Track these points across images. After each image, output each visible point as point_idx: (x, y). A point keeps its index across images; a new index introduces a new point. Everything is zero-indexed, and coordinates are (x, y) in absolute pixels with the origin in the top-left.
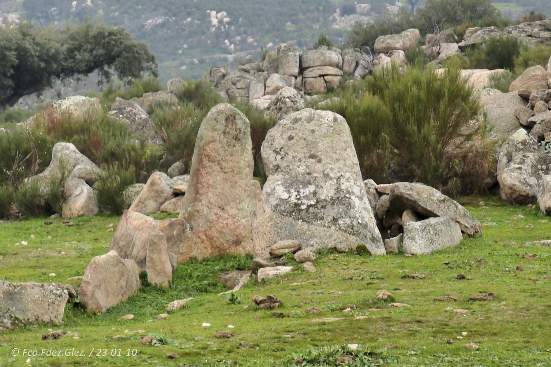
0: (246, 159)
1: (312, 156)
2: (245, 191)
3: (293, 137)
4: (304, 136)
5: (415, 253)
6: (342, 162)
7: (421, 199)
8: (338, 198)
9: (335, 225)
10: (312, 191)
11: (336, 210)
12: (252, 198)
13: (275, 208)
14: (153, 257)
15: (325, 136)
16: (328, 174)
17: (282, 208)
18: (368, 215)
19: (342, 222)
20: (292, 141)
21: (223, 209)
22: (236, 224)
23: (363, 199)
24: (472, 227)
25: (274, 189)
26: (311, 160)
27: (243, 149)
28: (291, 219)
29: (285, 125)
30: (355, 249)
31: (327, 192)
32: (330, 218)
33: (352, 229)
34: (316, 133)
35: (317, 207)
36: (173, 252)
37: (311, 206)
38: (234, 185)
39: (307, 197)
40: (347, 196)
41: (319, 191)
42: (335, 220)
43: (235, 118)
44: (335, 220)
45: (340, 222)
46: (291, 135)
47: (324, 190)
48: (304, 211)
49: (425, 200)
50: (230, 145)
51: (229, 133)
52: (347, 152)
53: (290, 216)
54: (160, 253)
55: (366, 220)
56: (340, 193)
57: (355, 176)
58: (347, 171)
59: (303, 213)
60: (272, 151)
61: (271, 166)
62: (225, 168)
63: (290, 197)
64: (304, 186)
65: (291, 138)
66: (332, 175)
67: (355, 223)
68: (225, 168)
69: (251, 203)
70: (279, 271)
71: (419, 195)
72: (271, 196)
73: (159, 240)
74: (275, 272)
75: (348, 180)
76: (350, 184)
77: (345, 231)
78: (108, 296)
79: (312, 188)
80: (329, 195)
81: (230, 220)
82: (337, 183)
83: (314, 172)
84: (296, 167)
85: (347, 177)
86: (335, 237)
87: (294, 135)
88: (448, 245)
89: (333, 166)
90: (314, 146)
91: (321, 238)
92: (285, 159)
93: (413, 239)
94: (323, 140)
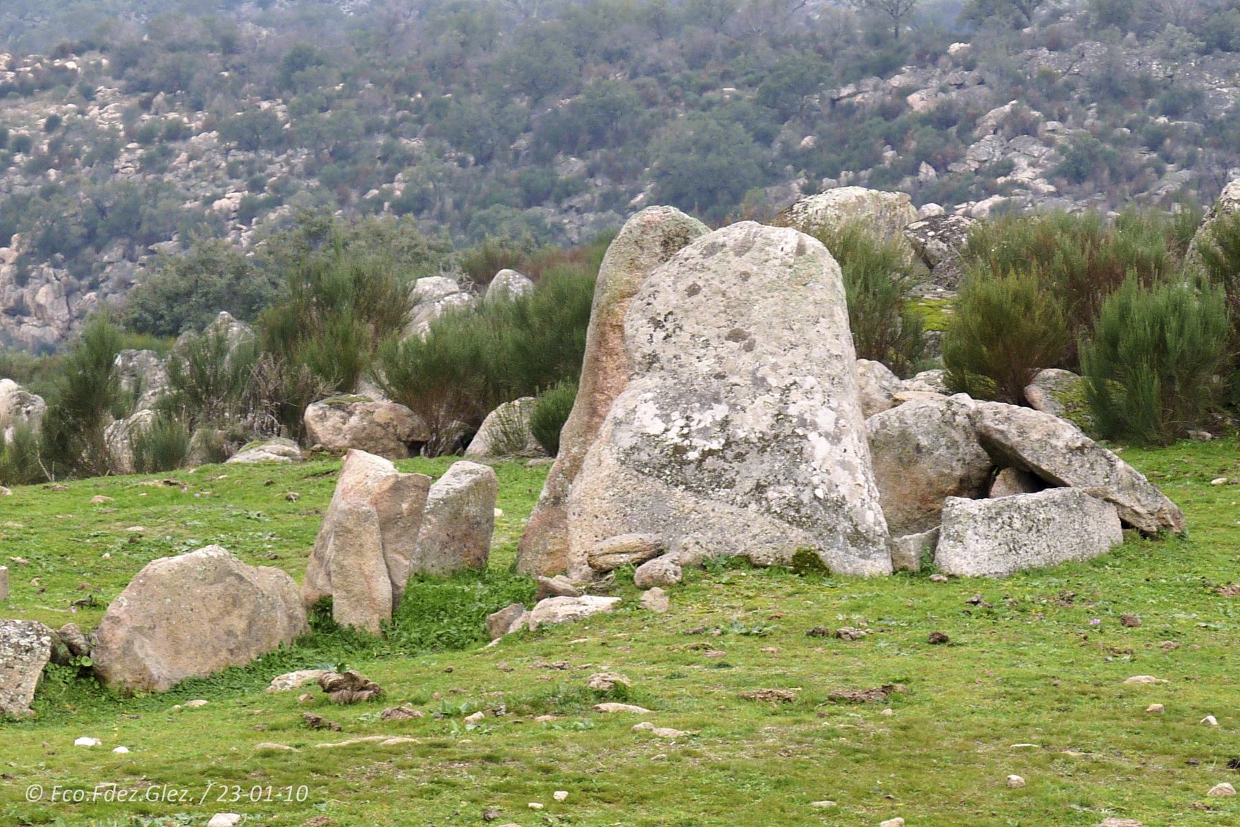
1: (736, 336)
3: (700, 288)
4: (723, 287)
5: (958, 573)
6: (802, 350)
7: (1027, 443)
8: (776, 436)
9: (758, 501)
10: (718, 418)
11: (766, 466)
13: (628, 455)
14: (345, 563)
15: (772, 287)
16: (763, 379)
17: (644, 457)
18: (849, 480)
19: (776, 495)
20: (695, 299)
23: (839, 440)
25: (634, 411)
26: (731, 344)
28: (659, 484)
29: (686, 259)
30: (790, 560)
31: (754, 420)
32: (749, 484)
33: (798, 511)
34: (753, 279)
35: (724, 458)
36: (400, 553)
37: (711, 452)
39: (705, 432)
40: (800, 431)
41: (736, 418)
42: (760, 488)
44: (760, 488)
45: (771, 494)
46: (695, 284)
47: (749, 416)
48: (693, 466)
49: (1036, 445)
53: (659, 477)
54: (359, 553)
55: (843, 490)
56: (782, 424)
57: (827, 385)
58: (809, 373)
59: (689, 471)
60: (645, 321)
63: (666, 430)
64: (702, 405)
65: (693, 291)
66: (772, 381)
67: (805, 498)
70: (582, 608)
71: (1022, 433)
72: (624, 427)
73: (358, 524)
75: (808, 394)
76: (812, 402)
77: (781, 517)
78: (178, 652)
79: (720, 411)
80: (757, 429)
82: (781, 400)
83: (732, 372)
84: (694, 360)
85: (807, 386)
86: (755, 531)
87: (700, 283)
88: (1068, 554)
90: (744, 311)
91: (722, 530)
92: (673, 339)
93: (959, 539)
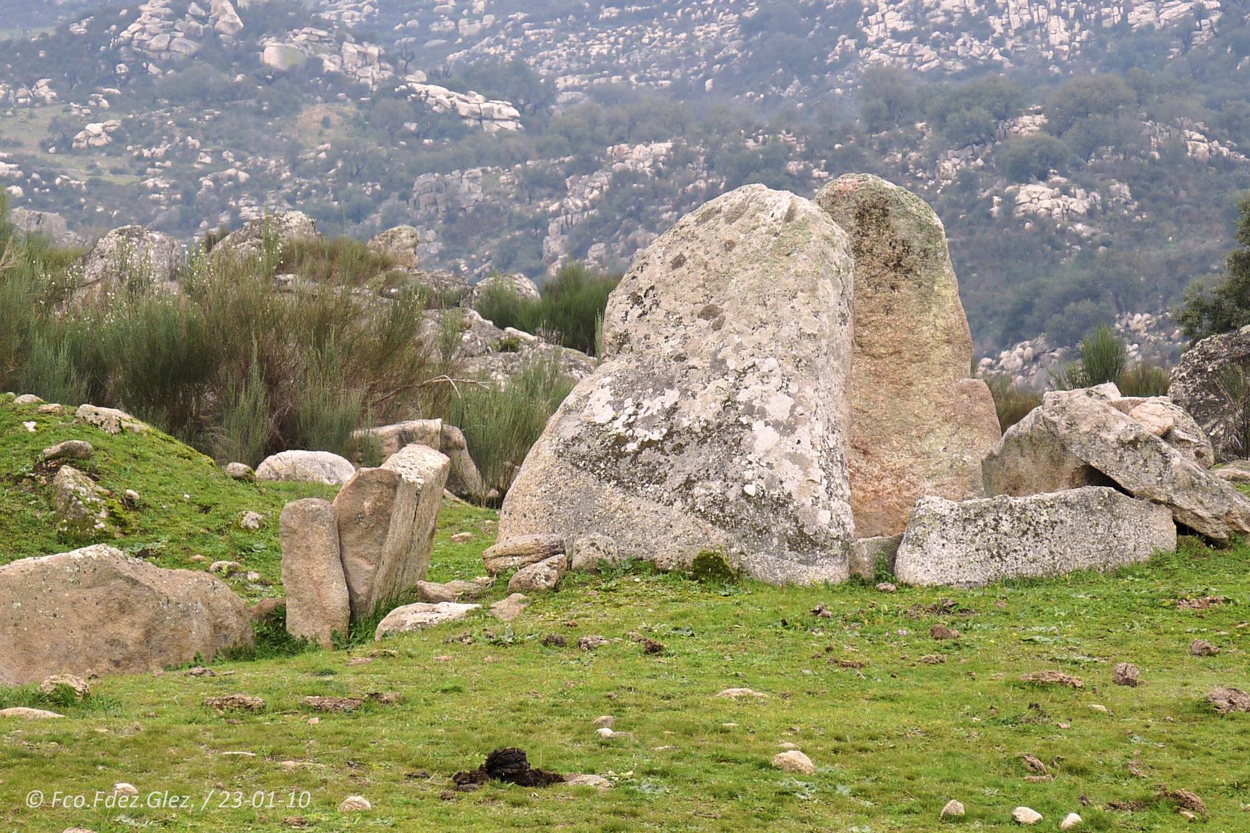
0: (940, 322)
1: (709, 313)
2: (939, 405)
3: (685, 259)
4: (706, 258)
5: (911, 581)
6: (771, 329)
7: (1074, 436)
8: (720, 425)
9: (684, 499)
10: (667, 406)
11: (701, 460)
12: (960, 425)
13: (567, 446)
14: (294, 567)
15: (757, 258)
16: (723, 361)
17: (583, 449)
18: (799, 475)
19: (703, 491)
20: (678, 272)
21: (865, 453)
22: (906, 494)
23: (793, 430)
24: (1217, 518)
25: (587, 397)
26: (703, 323)
27: (927, 296)
28: (591, 480)
29: (682, 227)
30: (691, 564)
31: (701, 409)
32: (680, 479)
33: (722, 510)
34: (738, 249)
35: (662, 450)
36: (362, 556)
37: (650, 444)
38: (903, 389)
39: (650, 422)
40: (744, 420)
41: (685, 405)
42: (689, 483)
43: (885, 214)
44: (689, 483)
45: (698, 490)
46: (681, 255)
47: (698, 404)
48: (629, 458)
49: (1084, 439)
50: (880, 284)
51: (870, 251)
52: (795, 302)
53: (592, 471)
54: (308, 557)
55: (789, 487)
56: (729, 412)
57: (790, 368)
58: (772, 354)
59: (624, 463)
60: (625, 297)
61: (608, 336)
62: (871, 345)
63: (615, 419)
64: (655, 390)
65: (678, 263)
66: (731, 364)
67: (732, 495)
68: (871, 345)
69: (955, 439)
70: (433, 616)
71: (1071, 425)
72: (574, 415)
73: (303, 523)
74: (420, 617)
75: (764, 378)
76: (766, 387)
77: (705, 516)
78: (30, 662)
79: (671, 397)
80: (703, 416)
81: (887, 482)
82: (734, 385)
83: (694, 354)
84: (662, 339)
85: (765, 369)
86: (678, 532)
87: (686, 254)
88: (1083, 563)
89: (745, 340)
90: (721, 284)
91: (644, 530)
92: (648, 317)
93: (918, 543)
94: (746, 270)
